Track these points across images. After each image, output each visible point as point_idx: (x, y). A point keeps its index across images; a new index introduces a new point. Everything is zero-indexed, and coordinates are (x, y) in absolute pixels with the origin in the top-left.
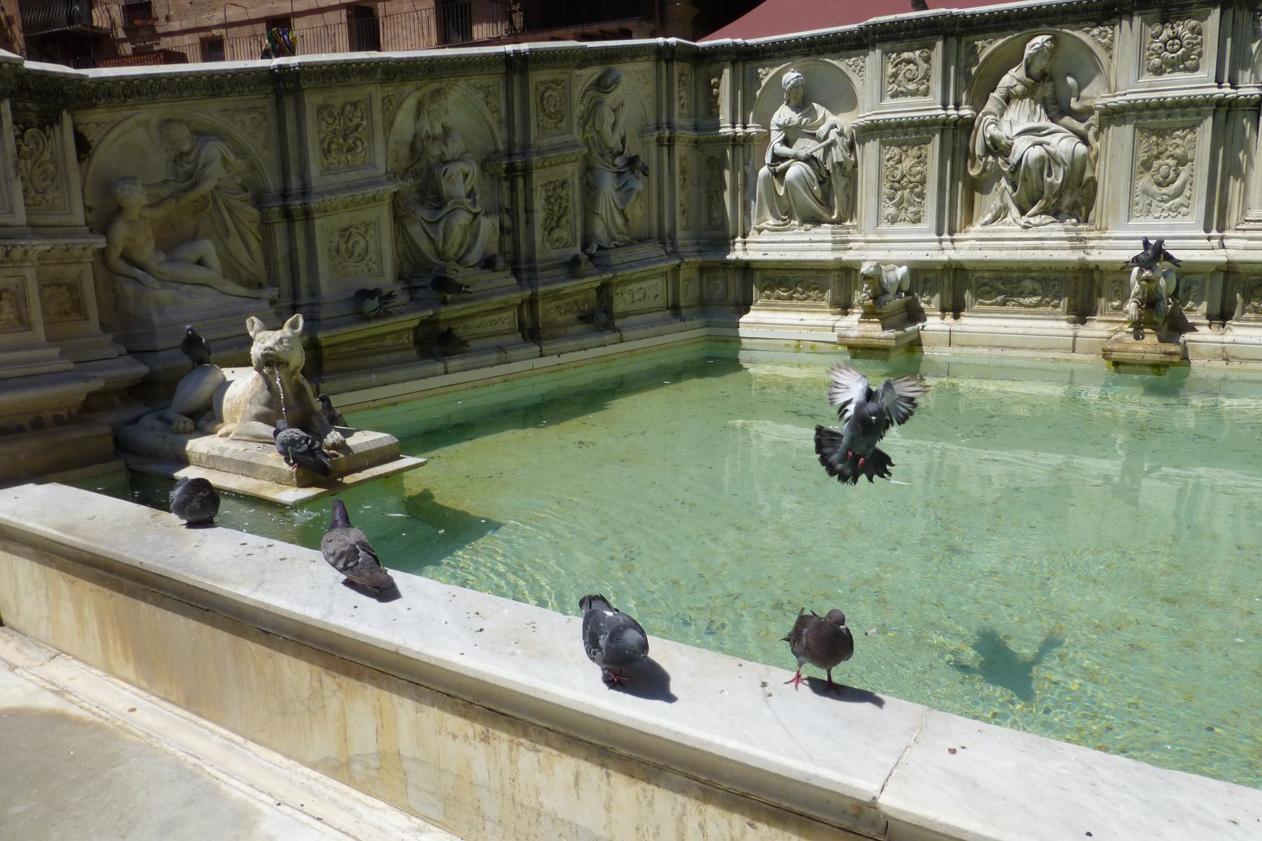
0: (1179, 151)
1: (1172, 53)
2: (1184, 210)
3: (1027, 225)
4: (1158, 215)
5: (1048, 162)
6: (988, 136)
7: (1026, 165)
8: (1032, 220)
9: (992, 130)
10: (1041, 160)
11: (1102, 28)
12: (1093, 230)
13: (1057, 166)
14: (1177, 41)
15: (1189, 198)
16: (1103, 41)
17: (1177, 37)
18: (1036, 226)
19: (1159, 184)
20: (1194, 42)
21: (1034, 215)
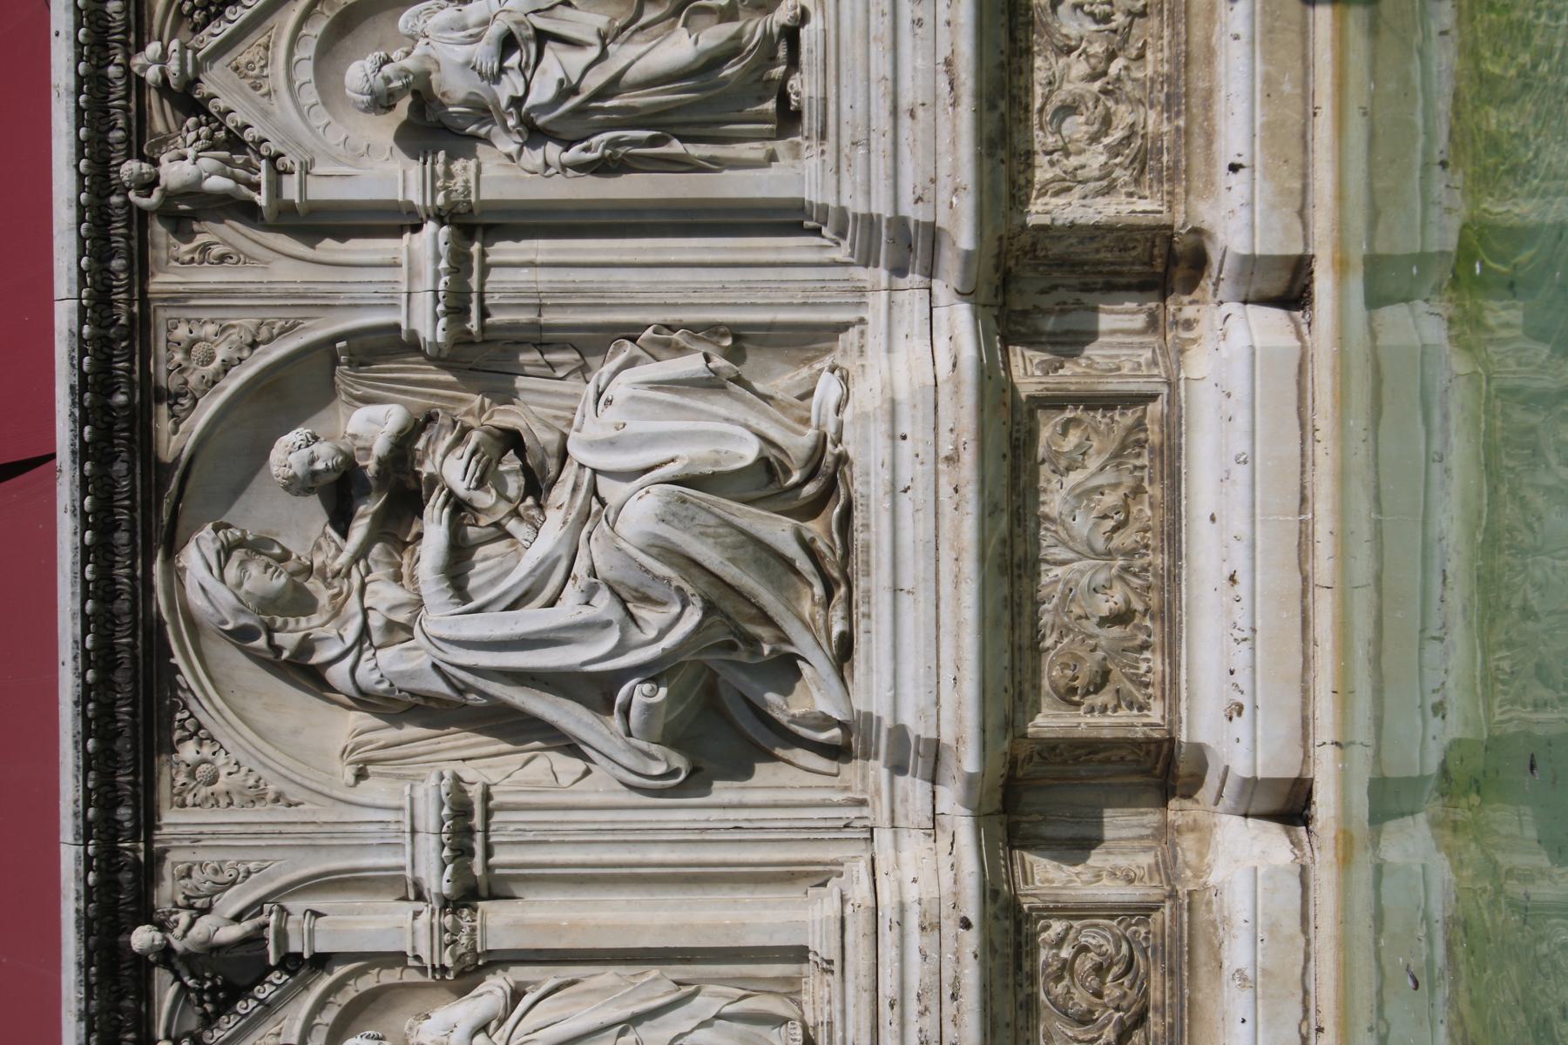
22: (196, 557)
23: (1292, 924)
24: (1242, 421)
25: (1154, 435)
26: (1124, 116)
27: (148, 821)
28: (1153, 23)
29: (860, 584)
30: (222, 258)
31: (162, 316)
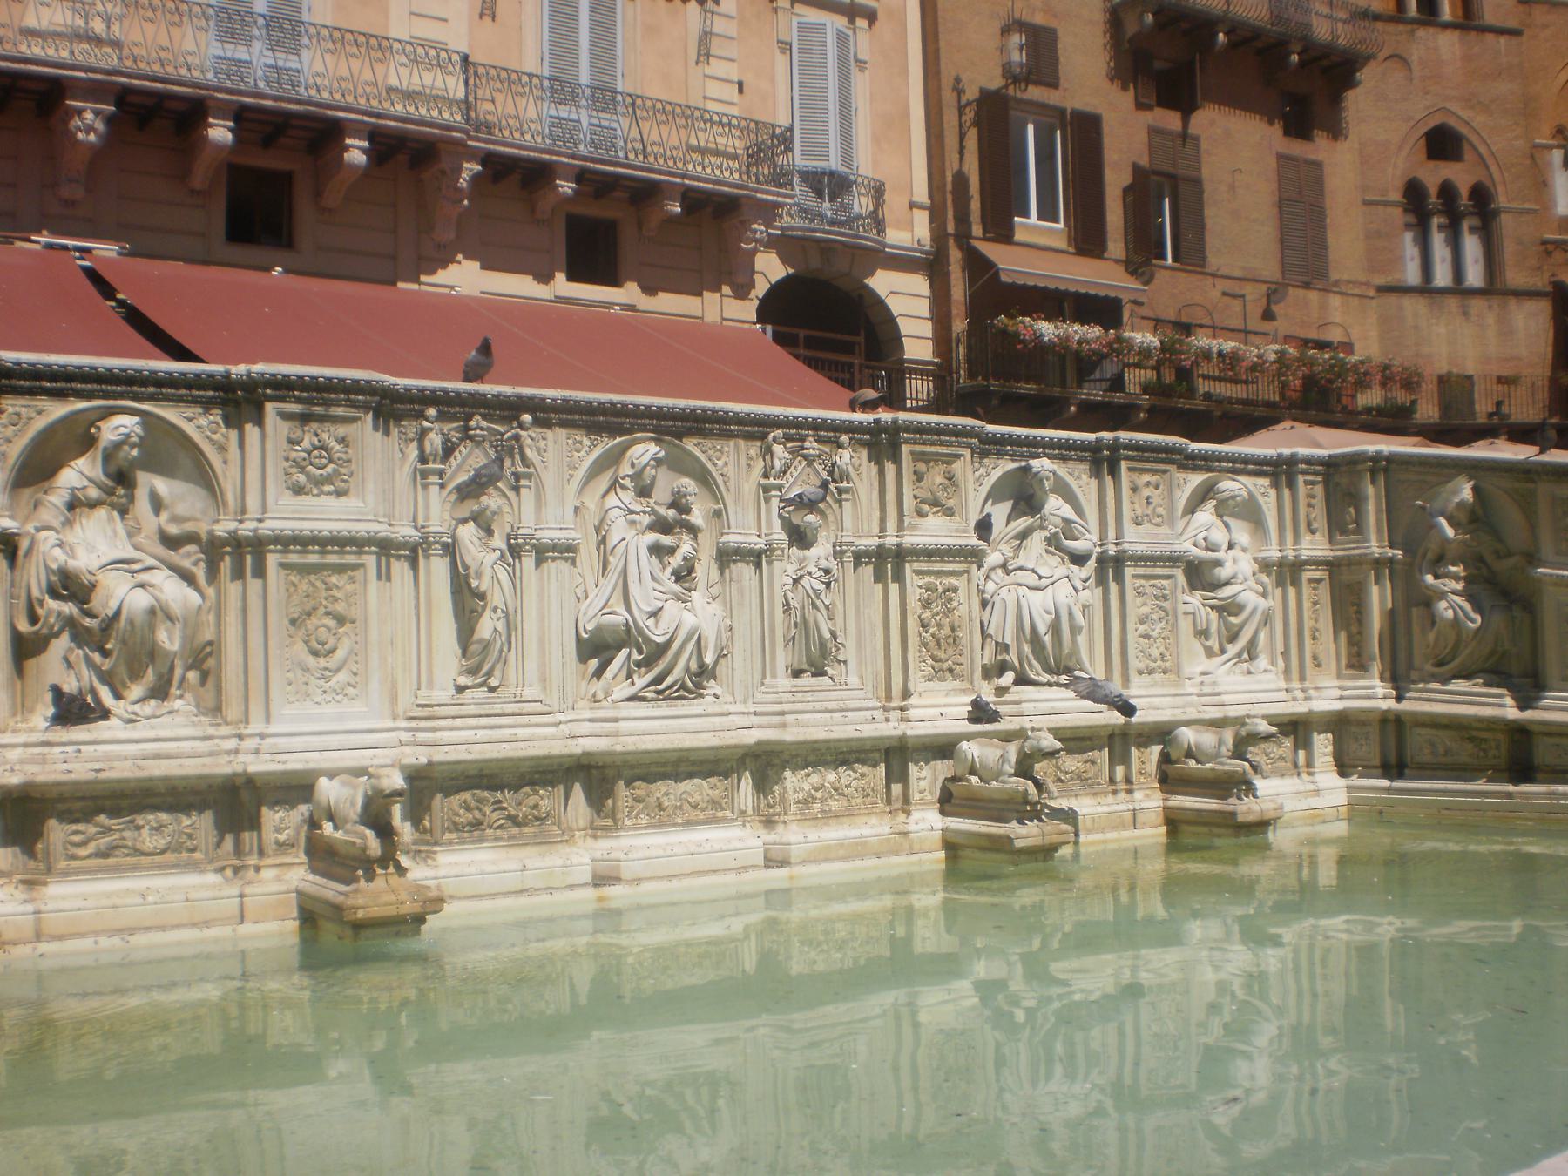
0: (340, 608)
1: (319, 468)
2: (350, 691)
3: (134, 717)
4: (319, 699)
5: (158, 613)
6: (54, 566)
7: (131, 622)
8: (136, 708)
9: (59, 557)
10: (152, 612)
11: (211, 418)
12: (219, 725)
13: (169, 624)
14: (324, 453)
15: (355, 674)
16: (214, 437)
17: (321, 448)
18: (147, 718)
19: (315, 653)
20: (343, 456)
21: (141, 700)
22: (653, 449)
23: (571, 881)
24: (731, 846)
25: (720, 814)
26: (819, 794)
27: (564, 424)
28: (845, 803)
29: (663, 703)
30: (749, 465)
31: (732, 443)
